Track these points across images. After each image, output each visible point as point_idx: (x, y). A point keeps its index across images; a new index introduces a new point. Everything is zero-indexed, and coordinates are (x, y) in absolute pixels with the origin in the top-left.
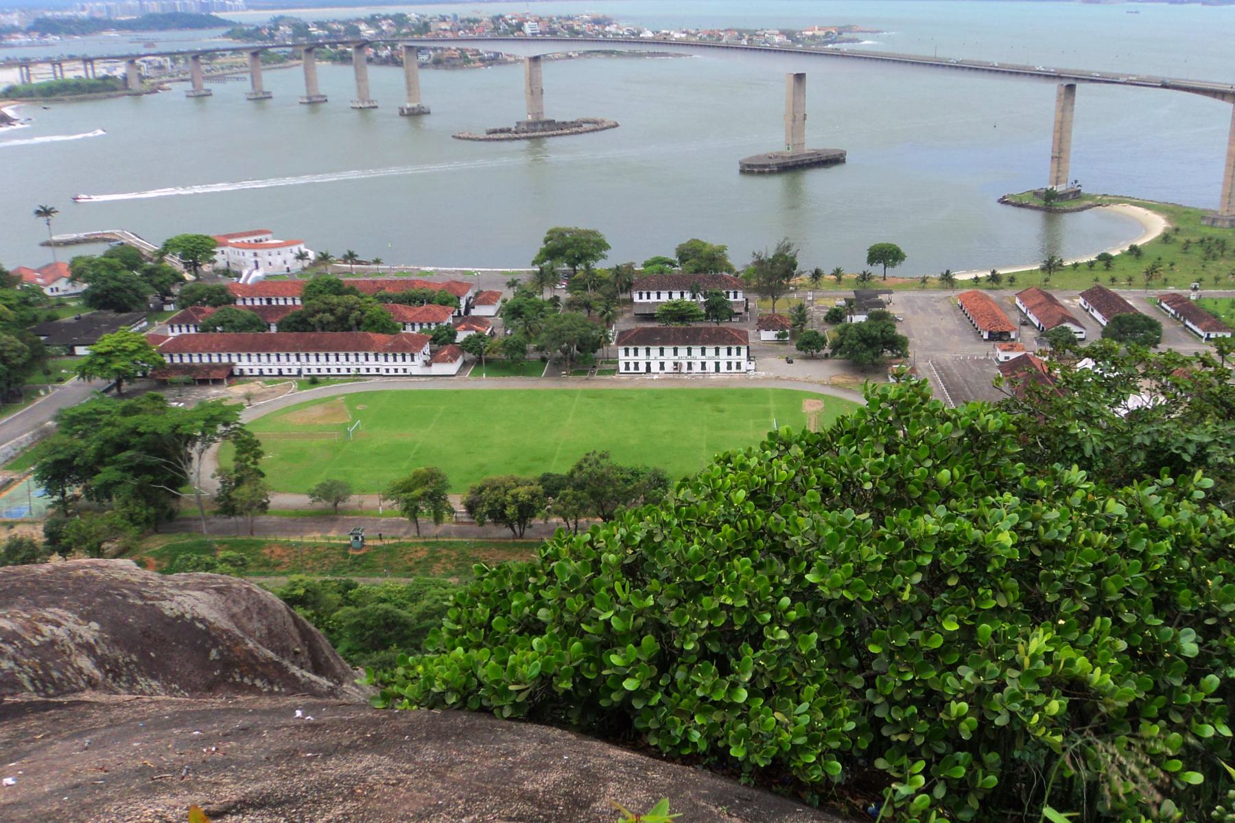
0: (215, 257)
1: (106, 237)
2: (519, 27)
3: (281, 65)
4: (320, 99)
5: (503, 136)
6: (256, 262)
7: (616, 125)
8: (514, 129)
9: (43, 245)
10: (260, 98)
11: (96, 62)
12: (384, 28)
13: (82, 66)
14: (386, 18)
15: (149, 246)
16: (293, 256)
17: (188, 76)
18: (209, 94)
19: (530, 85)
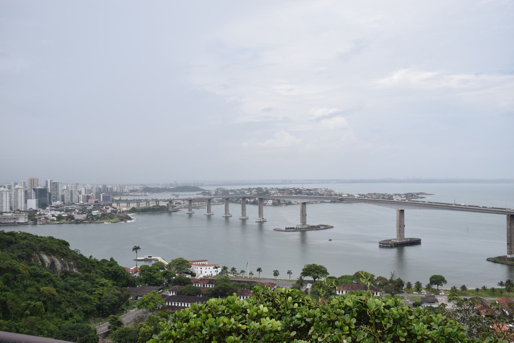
5: (291, 230)
7: (332, 227)
8: (295, 228)
9: (134, 260)
14: (254, 189)
19: (302, 212)
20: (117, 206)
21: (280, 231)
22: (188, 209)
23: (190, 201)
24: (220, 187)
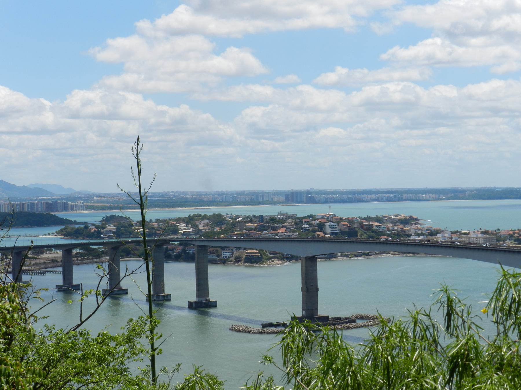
2: (321, 227)
12: (201, 227)
14: (205, 217)
19: (306, 283)
21: (245, 332)
24: (117, 213)
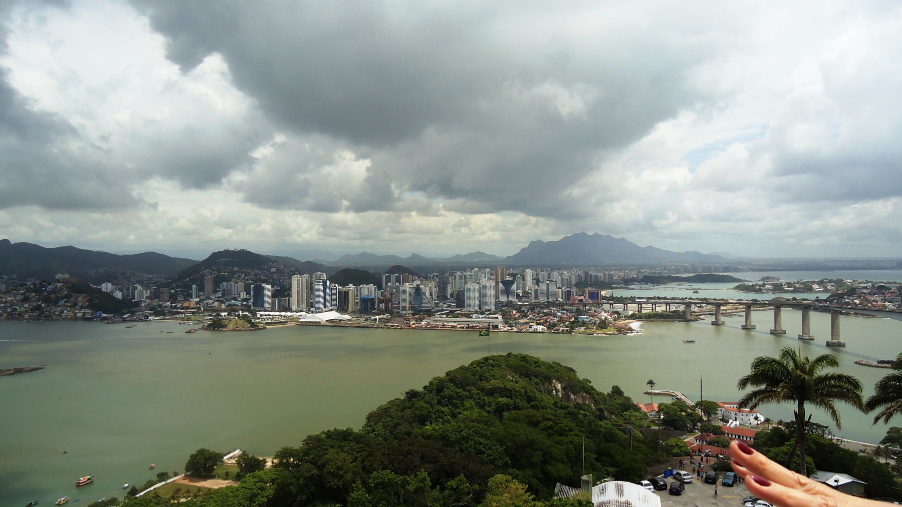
0: (718, 412)
1: (671, 393)
3: (763, 309)
4: (782, 332)
6: (736, 418)
9: (645, 393)
10: (747, 328)
11: (671, 305)
13: (651, 305)
15: (691, 403)
16: (753, 417)
17: (714, 312)
18: (723, 324)
20: (610, 308)
22: (714, 317)
23: (718, 305)
